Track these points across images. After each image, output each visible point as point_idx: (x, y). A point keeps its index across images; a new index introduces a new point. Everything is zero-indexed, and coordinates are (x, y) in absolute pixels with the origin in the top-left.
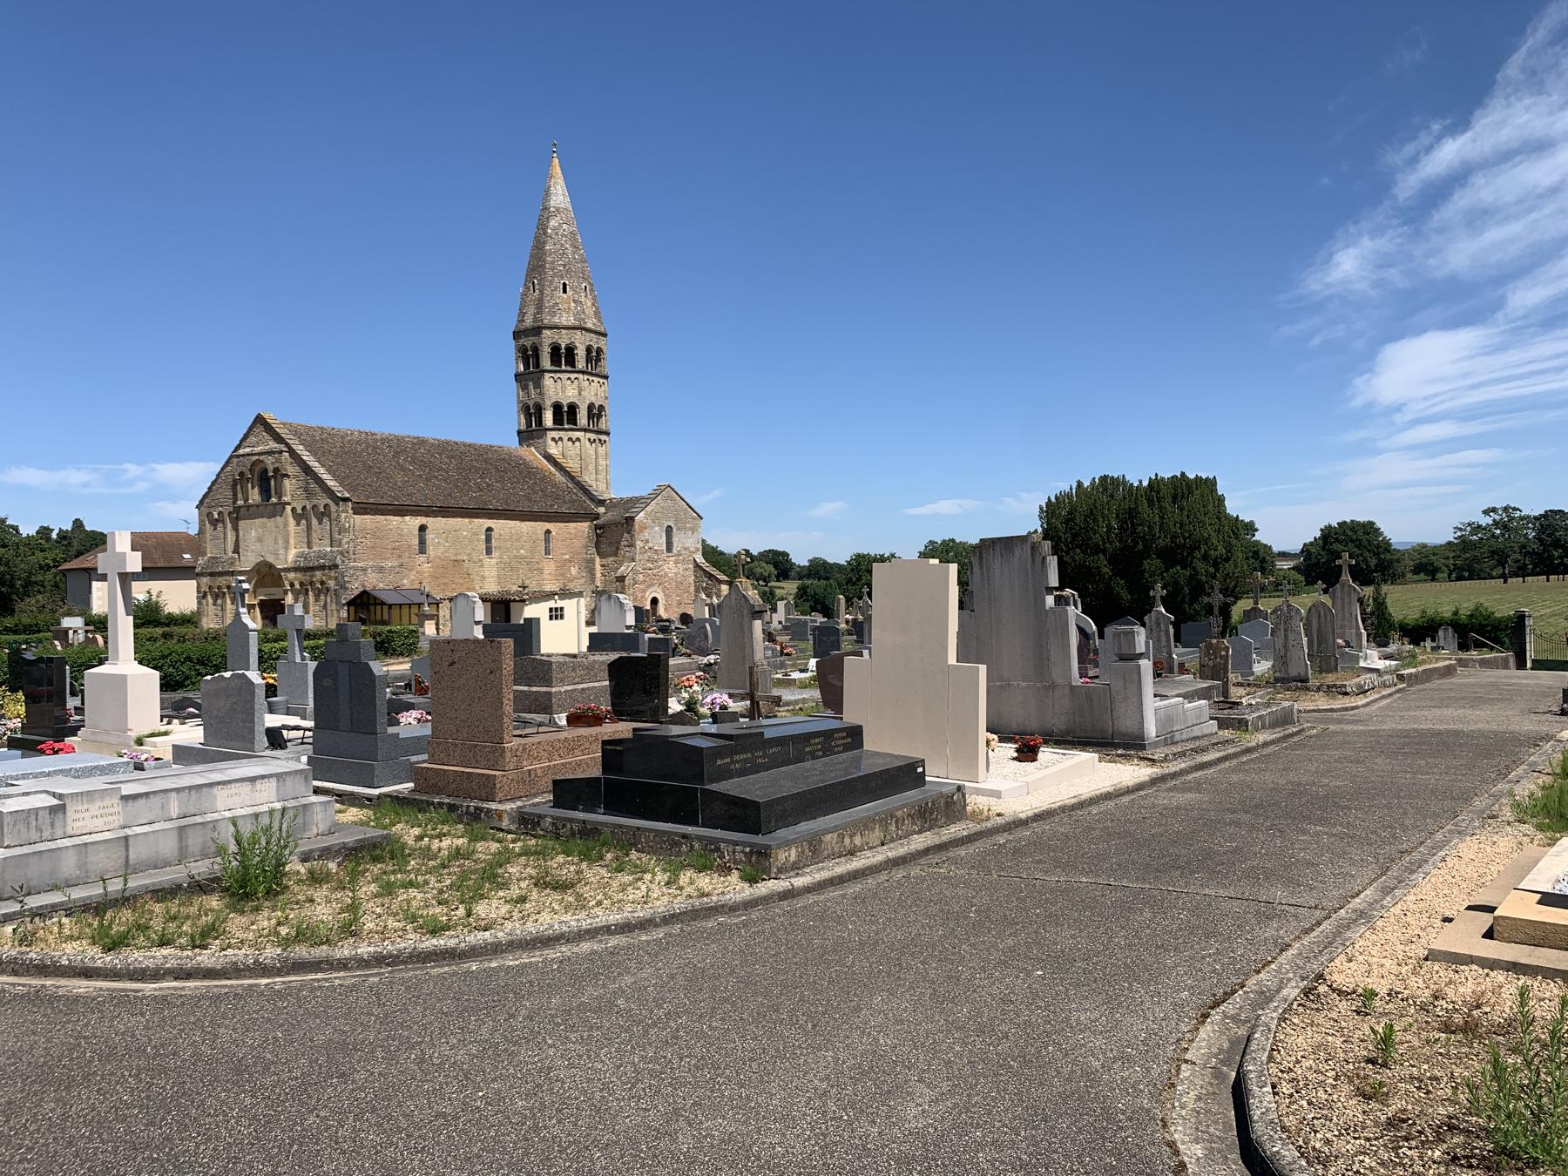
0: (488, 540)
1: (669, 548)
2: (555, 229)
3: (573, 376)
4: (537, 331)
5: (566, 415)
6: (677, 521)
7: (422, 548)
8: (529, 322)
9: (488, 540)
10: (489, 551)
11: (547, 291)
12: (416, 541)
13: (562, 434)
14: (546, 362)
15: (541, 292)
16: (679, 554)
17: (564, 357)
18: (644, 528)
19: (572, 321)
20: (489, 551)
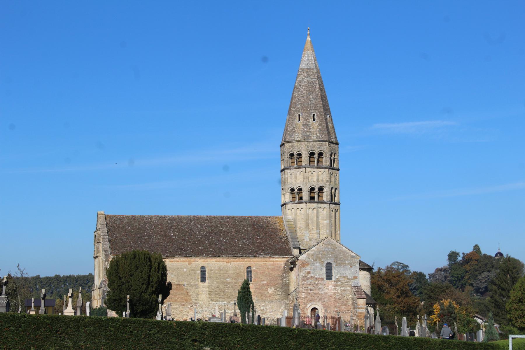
1: (329, 277)
6: (336, 258)
10: (203, 280)
16: (338, 280)
18: (305, 264)
20: (203, 280)
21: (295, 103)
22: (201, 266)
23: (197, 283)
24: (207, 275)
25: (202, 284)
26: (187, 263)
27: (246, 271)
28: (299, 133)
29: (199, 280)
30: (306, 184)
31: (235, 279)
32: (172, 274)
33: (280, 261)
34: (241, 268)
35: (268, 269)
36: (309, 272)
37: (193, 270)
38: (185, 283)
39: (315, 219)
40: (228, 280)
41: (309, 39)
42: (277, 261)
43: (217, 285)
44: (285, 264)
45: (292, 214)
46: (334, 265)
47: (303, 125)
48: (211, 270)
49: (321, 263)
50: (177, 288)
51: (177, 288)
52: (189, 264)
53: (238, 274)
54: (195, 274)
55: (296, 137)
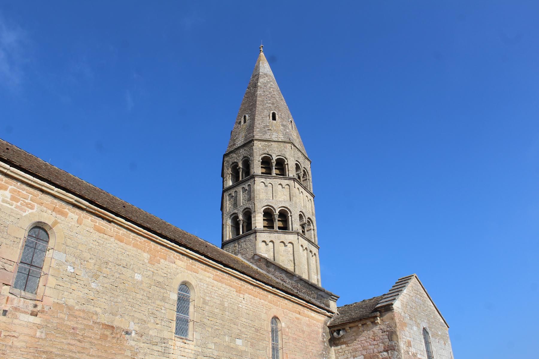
0: (183, 302)
2: (264, 83)
3: (285, 182)
4: (249, 143)
5: (277, 220)
7: (29, 273)
8: (240, 142)
9: (183, 302)
10: (182, 328)
11: (258, 118)
12: (15, 253)
13: (274, 236)
14: (257, 169)
15: (253, 119)
17: (275, 167)
19: (281, 138)
20: (182, 328)
21: (263, 101)
22: (180, 279)
23: (166, 334)
24: (192, 313)
25: (179, 343)
26: (146, 256)
27: (270, 329)
28: (277, 133)
29: (174, 324)
30: (296, 203)
31: (252, 345)
32: (95, 277)
33: (318, 321)
34: (263, 316)
35: (303, 332)
36: (409, 345)
37: (158, 284)
38: (132, 326)
39: (306, 267)
40: (239, 342)
41: (262, 54)
42: (312, 318)
43: (216, 353)
44: (324, 328)
45: (268, 251)
46: (430, 335)
47: (283, 125)
48: (205, 303)
49: (418, 325)
50: (104, 337)
51: (104, 337)
52: (151, 262)
53: (257, 330)
54: (164, 299)
55: (273, 136)
